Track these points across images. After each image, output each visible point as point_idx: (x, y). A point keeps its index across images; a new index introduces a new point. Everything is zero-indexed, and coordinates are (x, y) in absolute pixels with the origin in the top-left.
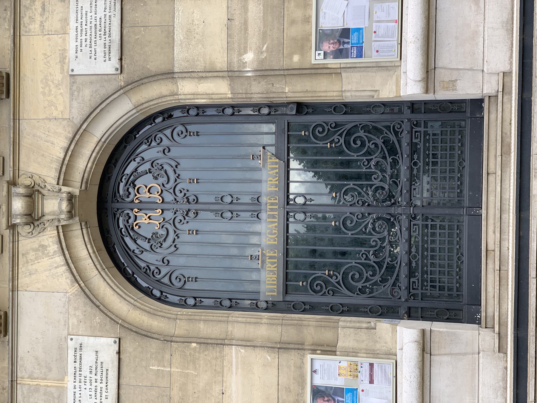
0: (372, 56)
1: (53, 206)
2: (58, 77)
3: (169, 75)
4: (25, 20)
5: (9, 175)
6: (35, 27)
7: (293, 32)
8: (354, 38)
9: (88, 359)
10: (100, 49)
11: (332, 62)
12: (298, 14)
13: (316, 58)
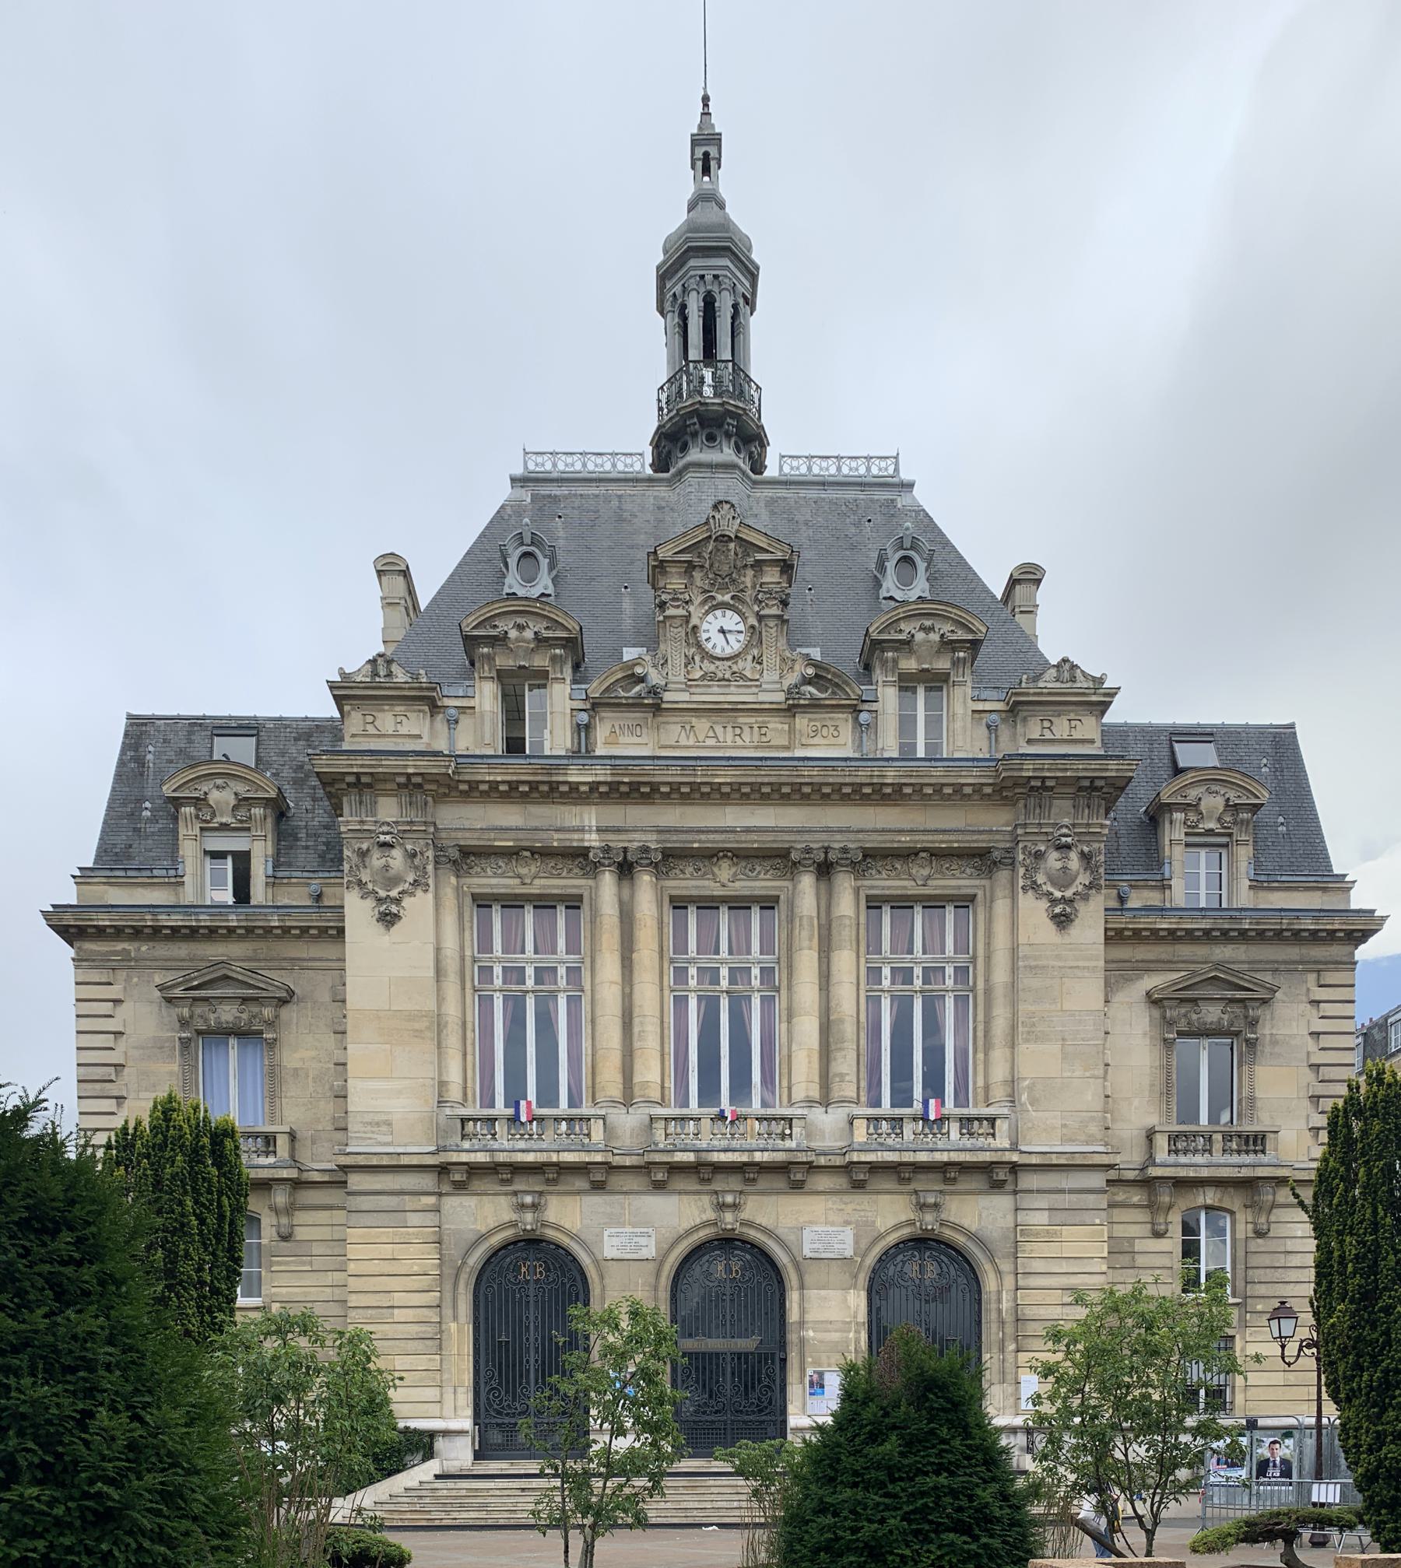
1: (729, 1217)
2: (801, 1220)
3: (802, 1287)
4: (834, 1198)
7: (824, 1357)
8: (819, 1390)
9: (643, 1241)
11: (807, 1379)
12: (833, 1361)
13: (809, 1371)
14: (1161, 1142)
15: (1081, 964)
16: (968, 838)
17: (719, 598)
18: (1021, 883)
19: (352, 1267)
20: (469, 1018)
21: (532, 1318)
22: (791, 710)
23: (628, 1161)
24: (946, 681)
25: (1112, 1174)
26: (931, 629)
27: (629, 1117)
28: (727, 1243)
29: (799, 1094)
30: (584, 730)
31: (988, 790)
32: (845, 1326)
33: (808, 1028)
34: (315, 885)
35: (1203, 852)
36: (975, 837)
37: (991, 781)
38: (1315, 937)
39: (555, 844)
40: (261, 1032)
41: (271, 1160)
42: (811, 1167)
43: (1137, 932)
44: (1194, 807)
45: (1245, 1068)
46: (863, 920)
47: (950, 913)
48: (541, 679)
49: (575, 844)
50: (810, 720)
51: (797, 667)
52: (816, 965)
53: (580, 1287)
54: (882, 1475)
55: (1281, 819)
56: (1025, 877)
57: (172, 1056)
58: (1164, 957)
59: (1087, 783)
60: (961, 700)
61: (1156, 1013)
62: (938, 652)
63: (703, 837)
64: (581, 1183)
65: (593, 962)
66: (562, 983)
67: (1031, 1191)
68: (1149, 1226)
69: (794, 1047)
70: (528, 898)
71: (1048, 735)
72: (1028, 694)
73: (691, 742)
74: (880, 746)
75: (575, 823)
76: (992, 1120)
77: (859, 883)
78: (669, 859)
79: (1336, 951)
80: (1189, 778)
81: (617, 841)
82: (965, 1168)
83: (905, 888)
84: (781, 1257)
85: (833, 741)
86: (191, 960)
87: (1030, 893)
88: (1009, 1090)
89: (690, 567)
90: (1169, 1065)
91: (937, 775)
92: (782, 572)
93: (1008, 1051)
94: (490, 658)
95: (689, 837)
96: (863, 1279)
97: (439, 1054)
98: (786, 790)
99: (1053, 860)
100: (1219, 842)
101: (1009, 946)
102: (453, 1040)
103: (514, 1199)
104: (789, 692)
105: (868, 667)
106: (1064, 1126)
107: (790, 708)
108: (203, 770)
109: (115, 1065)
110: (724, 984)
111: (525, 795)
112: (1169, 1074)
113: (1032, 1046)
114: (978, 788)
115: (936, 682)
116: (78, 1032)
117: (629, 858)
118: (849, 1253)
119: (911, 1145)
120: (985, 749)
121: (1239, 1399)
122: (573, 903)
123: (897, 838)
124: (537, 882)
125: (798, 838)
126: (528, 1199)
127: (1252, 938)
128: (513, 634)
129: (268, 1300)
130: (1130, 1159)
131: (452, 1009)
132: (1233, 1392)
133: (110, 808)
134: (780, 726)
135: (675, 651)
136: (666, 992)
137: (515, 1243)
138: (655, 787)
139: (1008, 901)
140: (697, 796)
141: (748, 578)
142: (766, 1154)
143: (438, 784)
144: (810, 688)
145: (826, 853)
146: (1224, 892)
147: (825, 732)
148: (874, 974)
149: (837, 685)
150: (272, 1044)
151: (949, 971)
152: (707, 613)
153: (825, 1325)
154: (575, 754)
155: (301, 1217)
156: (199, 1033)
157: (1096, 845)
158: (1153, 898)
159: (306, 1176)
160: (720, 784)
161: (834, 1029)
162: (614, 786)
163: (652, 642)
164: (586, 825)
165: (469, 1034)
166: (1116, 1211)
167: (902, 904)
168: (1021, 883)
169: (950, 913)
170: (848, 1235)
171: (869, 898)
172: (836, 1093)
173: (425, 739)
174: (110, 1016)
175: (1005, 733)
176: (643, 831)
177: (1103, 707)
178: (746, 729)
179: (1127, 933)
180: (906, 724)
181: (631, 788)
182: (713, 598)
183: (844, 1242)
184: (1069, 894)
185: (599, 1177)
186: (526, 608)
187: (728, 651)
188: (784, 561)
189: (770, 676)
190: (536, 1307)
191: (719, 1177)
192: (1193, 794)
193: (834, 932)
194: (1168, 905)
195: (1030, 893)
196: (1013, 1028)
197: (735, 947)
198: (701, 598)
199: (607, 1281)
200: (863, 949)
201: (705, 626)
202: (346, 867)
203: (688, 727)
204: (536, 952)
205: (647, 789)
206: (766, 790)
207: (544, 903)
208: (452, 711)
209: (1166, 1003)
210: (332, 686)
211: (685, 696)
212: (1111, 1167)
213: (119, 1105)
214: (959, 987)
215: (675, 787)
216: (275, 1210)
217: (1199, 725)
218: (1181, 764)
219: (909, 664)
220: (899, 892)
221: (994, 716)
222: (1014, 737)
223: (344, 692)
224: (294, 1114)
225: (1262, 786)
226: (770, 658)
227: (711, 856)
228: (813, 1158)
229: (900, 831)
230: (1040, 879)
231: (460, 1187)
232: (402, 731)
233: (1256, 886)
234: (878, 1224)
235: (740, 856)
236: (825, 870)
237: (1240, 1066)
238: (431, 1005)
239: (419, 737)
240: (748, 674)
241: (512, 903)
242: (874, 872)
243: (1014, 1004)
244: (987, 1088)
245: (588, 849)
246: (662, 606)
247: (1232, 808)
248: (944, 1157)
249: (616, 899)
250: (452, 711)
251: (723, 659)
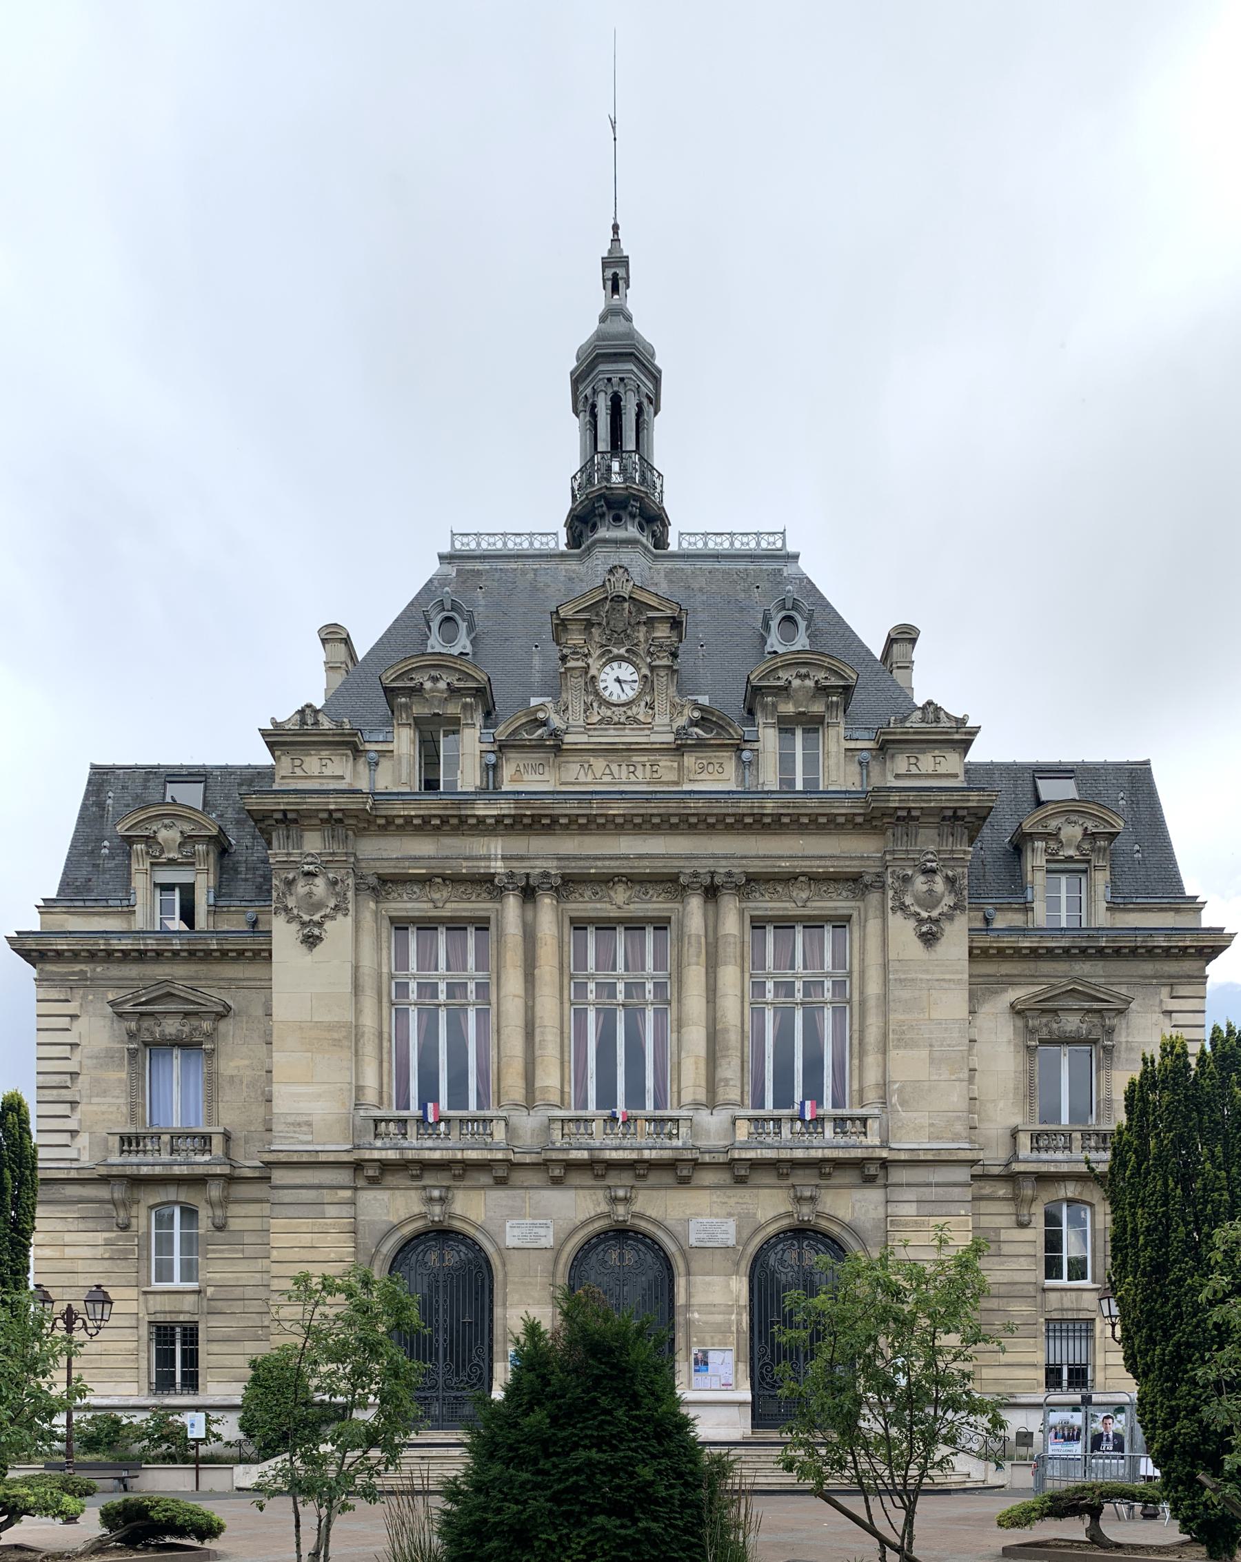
0: (694, 1377)
1: (621, 1209)
2: (688, 1212)
3: (688, 1273)
4: (719, 1192)
5: (638, 1184)
6: (715, 1198)
7: (708, 1338)
8: (704, 1368)
9: (542, 1231)
10: (701, 1236)
11: (693, 1357)
12: (716, 1340)
13: (695, 1350)
14: (1025, 1140)
15: (947, 977)
16: (842, 863)
17: (615, 651)
18: (890, 904)
19: (275, 1254)
20: (385, 1029)
21: (441, 1302)
22: (679, 749)
23: (528, 1159)
24: (822, 723)
25: (977, 1170)
26: (807, 676)
27: (531, 1119)
28: (622, 1233)
29: (687, 1097)
30: (492, 770)
31: (859, 820)
32: (728, 1309)
33: (696, 1037)
34: (251, 913)
35: (1064, 879)
36: (847, 863)
37: (862, 811)
38: (1167, 953)
40: (201, 1044)
41: (207, 1158)
42: (696, 1164)
43: (1001, 951)
44: (1054, 836)
45: (1103, 1073)
46: (748, 938)
47: (828, 932)
48: (454, 726)
50: (697, 758)
51: (686, 711)
52: (703, 979)
53: (485, 1271)
54: (532, 1450)
55: (1137, 847)
56: (893, 898)
57: (121, 1065)
58: (1027, 972)
59: (949, 813)
60: (834, 740)
61: (1020, 1023)
62: (814, 696)
63: (599, 863)
64: (485, 1179)
65: (498, 978)
66: (472, 997)
67: (901, 1185)
68: (1014, 1217)
69: (683, 1055)
70: (441, 921)
71: (914, 770)
72: (894, 733)
73: (589, 779)
74: (761, 781)
75: (483, 852)
76: (864, 1120)
77: (744, 905)
78: (568, 883)
79: (1188, 966)
80: (1049, 809)
81: (520, 868)
82: (839, 1164)
83: (786, 909)
84: (671, 1247)
86: (141, 979)
87: (899, 913)
88: (881, 1093)
89: (589, 624)
90: (1031, 1071)
91: (813, 805)
92: (672, 628)
93: (880, 1057)
94: (407, 707)
95: (587, 864)
96: (745, 1266)
97: (357, 1062)
98: (674, 820)
99: (920, 884)
100: (1079, 868)
101: (880, 961)
102: (369, 1049)
103: (423, 1193)
104: (678, 733)
105: (751, 712)
106: (931, 1125)
108: (152, 812)
109: (71, 1073)
110: (621, 997)
111: (437, 828)
112: (1031, 1079)
113: (901, 1052)
114: (850, 818)
115: (812, 724)
116: (38, 1044)
117: (531, 882)
118: (732, 1242)
119: (789, 1142)
120: (858, 783)
121: (1100, 1377)
122: (482, 925)
123: (778, 863)
124: (448, 905)
125: (687, 864)
126: (436, 1193)
127: (1108, 955)
128: (428, 685)
129: (204, 1284)
130: (994, 1156)
131: (368, 1021)
132: (1094, 1371)
133: (73, 847)
134: (669, 764)
135: (575, 699)
136: (566, 1005)
137: (426, 1233)
138: (554, 819)
139: (879, 921)
140: (594, 826)
141: (641, 634)
142: (654, 1152)
143: (354, 820)
144: (696, 730)
145: (712, 878)
146: (1084, 913)
147: (711, 768)
148: (759, 987)
149: (721, 727)
150: (211, 1054)
151: (828, 984)
152: (605, 665)
153: (710, 1308)
154: (482, 791)
155: (234, 1209)
156: (146, 1044)
157: (960, 870)
158: (1017, 919)
159: (238, 1172)
160: (614, 815)
161: (720, 1037)
162: (517, 818)
163: (554, 690)
164: (494, 853)
165: (385, 1044)
166: (983, 1203)
167: (784, 924)
168: (890, 904)
169: (828, 932)
170: (731, 1225)
171: (753, 919)
172: (721, 1098)
173: (348, 780)
174: (68, 1030)
175: (875, 769)
177: (965, 745)
178: (640, 768)
179: (991, 951)
180: (786, 761)
181: (532, 821)
182: (610, 651)
183: (727, 1233)
184: (935, 914)
185: (500, 1173)
186: (441, 664)
187: (624, 698)
188: (674, 618)
189: (661, 720)
190: (445, 1293)
191: (612, 1173)
192: (1053, 824)
193: (721, 950)
194: (1031, 926)
195: (899, 913)
196: (885, 1035)
197: (629, 962)
198: (598, 652)
199: (509, 1267)
200: (748, 964)
201: (603, 676)
202: (274, 894)
203: (586, 766)
204: (448, 969)
205: (548, 821)
206: (656, 820)
207: (456, 925)
208: (373, 755)
209: (1028, 1013)
210: (264, 733)
211: (584, 738)
212: (974, 1162)
213: (73, 1109)
214: (837, 999)
215: (573, 819)
216: (211, 1204)
217: (1060, 763)
218: (1043, 798)
219: (788, 708)
220: (781, 913)
221: (865, 754)
222: (884, 775)
223: (276, 739)
224: (229, 1116)
225: (1118, 815)
226: (662, 704)
227: (607, 880)
228: (698, 1155)
229: (781, 857)
230: (908, 900)
231: (374, 1182)
232: (328, 772)
233: (1113, 907)
234: (759, 1215)
235: (632, 880)
236: (712, 892)
237: (1098, 1070)
238: (349, 1016)
239: (342, 778)
240: (641, 717)
241: (427, 925)
242: (757, 895)
243: (885, 1015)
244: (861, 1091)
245: (494, 874)
246: (564, 659)
247: (1089, 836)
248: (819, 1154)
249: (519, 921)
250: (373, 755)
251: (619, 705)
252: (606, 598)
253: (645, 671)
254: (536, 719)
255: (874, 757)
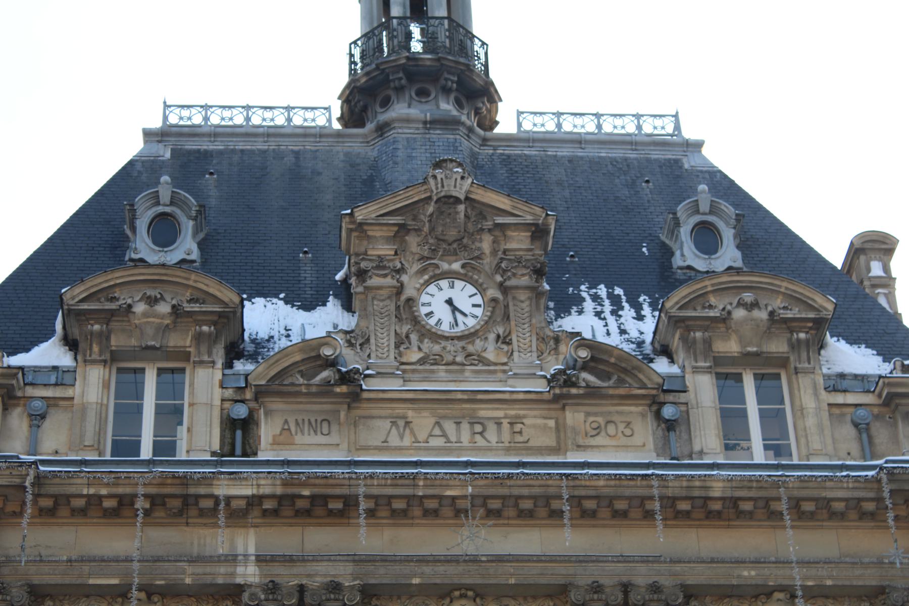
17: (445, 266)
26: (754, 305)
39: (188, 581)
49: (220, 581)
50: (588, 414)
51: (563, 348)
63: (427, 569)
73: (407, 441)
81: (289, 577)
85: (624, 441)
89: (403, 229)
92: (534, 238)
94: (104, 337)
107: (557, 399)
120: (855, 448)
128: (140, 308)
134: (540, 421)
141: (486, 244)
145: (626, 593)
147: (611, 429)
152: (427, 283)
160: (454, 498)
176: (330, 558)
181: (312, 502)
182: (437, 266)
188: (536, 225)
198: (416, 267)
201: (424, 298)
203: (401, 423)
219: (731, 347)
221: (861, 412)
240: (490, 355)
250: (38, 404)
251: (452, 339)
252: (430, 198)
253: (493, 292)
254: (319, 356)
255: (877, 417)
